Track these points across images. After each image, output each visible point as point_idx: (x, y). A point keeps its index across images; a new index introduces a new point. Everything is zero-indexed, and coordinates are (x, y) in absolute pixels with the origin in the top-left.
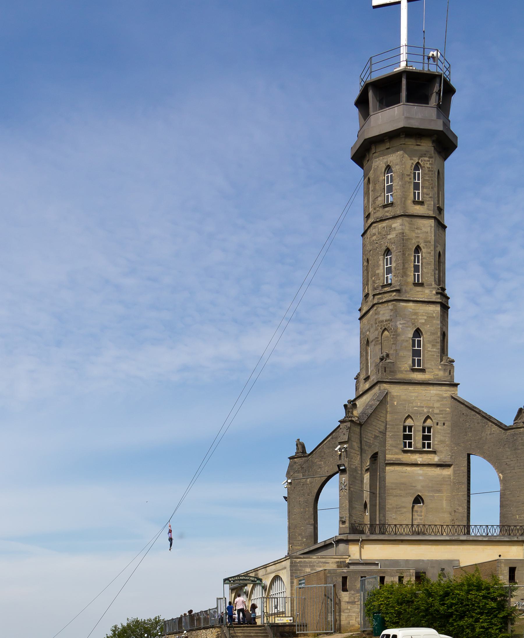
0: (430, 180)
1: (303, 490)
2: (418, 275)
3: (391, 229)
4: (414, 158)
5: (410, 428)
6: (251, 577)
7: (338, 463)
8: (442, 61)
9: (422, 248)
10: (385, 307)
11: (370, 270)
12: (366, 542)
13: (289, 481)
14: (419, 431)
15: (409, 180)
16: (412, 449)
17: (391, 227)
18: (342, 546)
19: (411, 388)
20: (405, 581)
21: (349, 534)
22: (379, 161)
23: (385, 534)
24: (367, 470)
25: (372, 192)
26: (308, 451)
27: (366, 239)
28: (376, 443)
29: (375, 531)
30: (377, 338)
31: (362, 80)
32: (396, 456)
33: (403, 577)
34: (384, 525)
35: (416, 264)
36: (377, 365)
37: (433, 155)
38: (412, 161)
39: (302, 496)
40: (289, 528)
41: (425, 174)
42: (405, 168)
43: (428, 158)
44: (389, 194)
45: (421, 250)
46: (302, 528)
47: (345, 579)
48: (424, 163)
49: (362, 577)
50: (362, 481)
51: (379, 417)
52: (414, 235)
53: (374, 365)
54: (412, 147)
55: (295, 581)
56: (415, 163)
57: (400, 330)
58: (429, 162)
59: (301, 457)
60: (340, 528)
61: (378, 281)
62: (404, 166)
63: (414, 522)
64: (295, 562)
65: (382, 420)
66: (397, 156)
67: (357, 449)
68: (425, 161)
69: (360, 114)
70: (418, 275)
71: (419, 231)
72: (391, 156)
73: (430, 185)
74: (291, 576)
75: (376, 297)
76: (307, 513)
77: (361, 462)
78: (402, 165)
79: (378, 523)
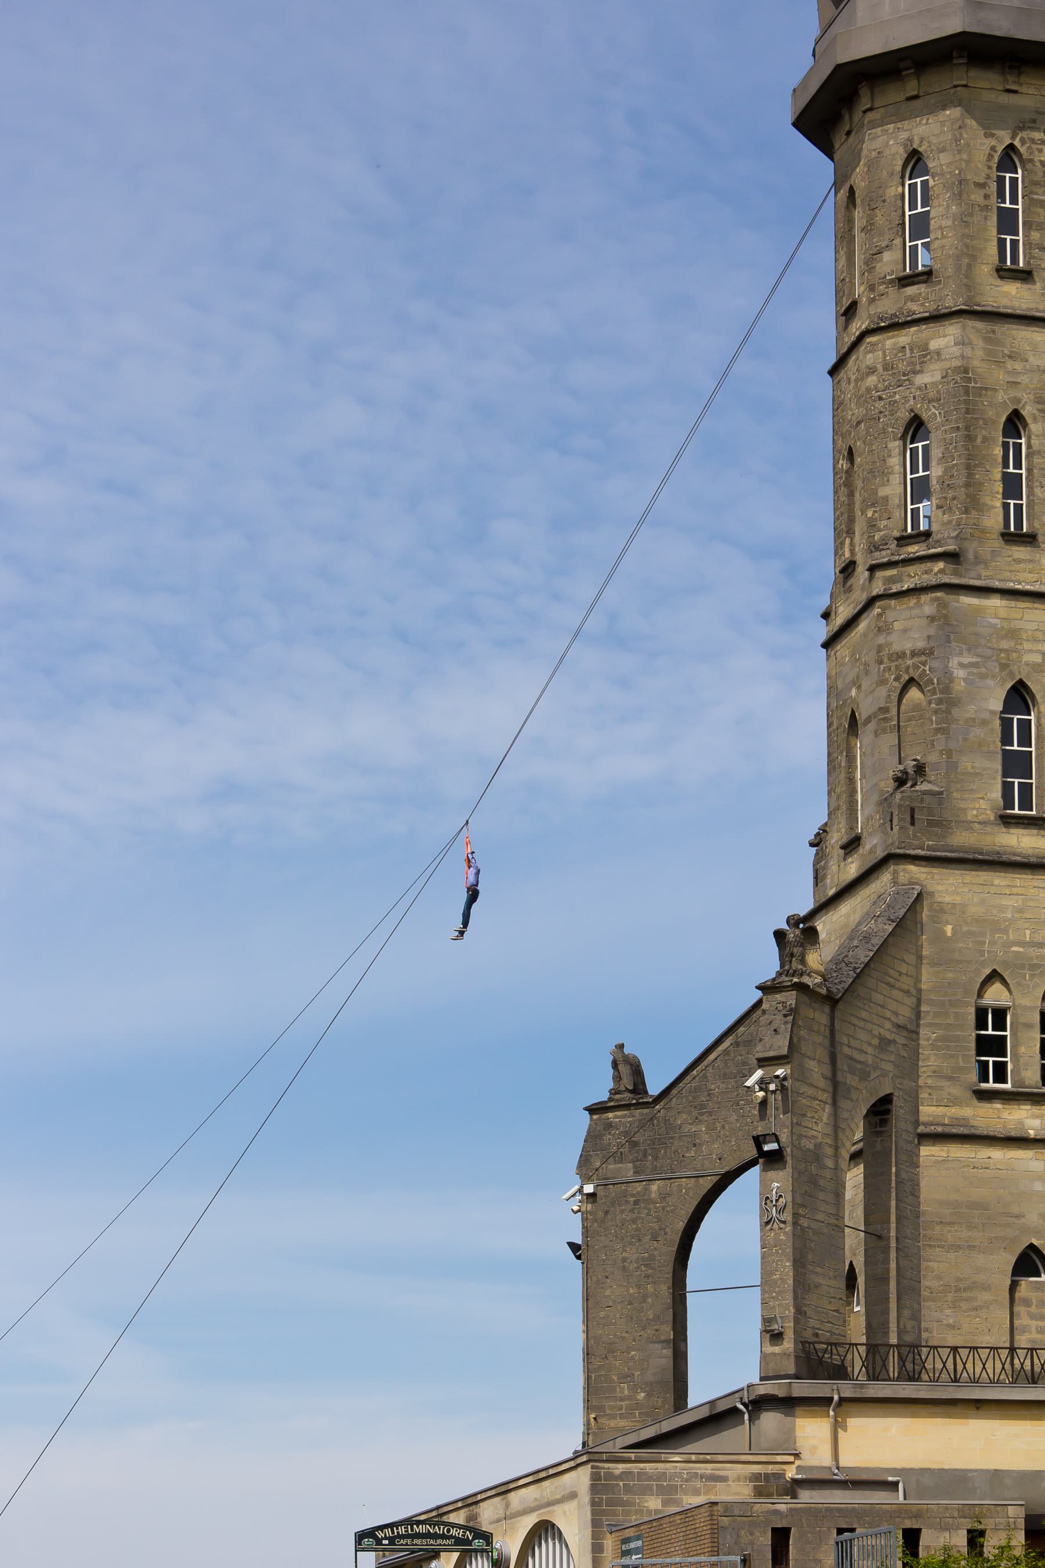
1: (634, 1221)
2: (1018, 508)
3: (925, 355)
4: (1000, 133)
5: (1000, 1016)
6: (453, 1525)
7: (755, 1129)
9: (1029, 420)
10: (911, 608)
11: (859, 484)
12: (853, 1408)
13: (589, 1189)
14: (1029, 1026)
16: (1008, 1086)
17: (925, 347)
18: (770, 1420)
19: (1000, 879)
20: (991, 1545)
21: (797, 1377)
22: (885, 136)
23: (919, 1379)
24: (855, 1157)
25: (863, 234)
26: (654, 1086)
27: (843, 384)
28: (883, 1065)
29: (884, 1371)
30: (886, 710)
32: (954, 1111)
33: (982, 1533)
34: (915, 1347)
35: (1011, 470)
36: (885, 802)
38: (993, 142)
39: (631, 1243)
40: (588, 1354)
41: (1037, 183)
42: (968, 162)
43: (1042, 134)
44: (919, 242)
45: (1025, 425)
46: (633, 1353)
47: (781, 1537)
48: (1029, 148)
49: (840, 1531)
50: (838, 1194)
51: (895, 974)
52: (1002, 377)
53: (875, 798)
54: (992, 96)
55: (609, 1543)
56: (1000, 148)
57: (959, 686)
59: (627, 1107)
60: (764, 1357)
61: (884, 523)
62: (965, 157)
63: (1017, 1338)
64: (609, 1476)
65: (905, 987)
66: (943, 123)
67: (822, 1083)
68: (1033, 141)
70: (1018, 508)
71: (1018, 366)
72: (924, 121)
74: (596, 1523)
75: (880, 574)
76: (650, 1300)
77: (836, 1128)
78: (960, 152)
79: (893, 1340)
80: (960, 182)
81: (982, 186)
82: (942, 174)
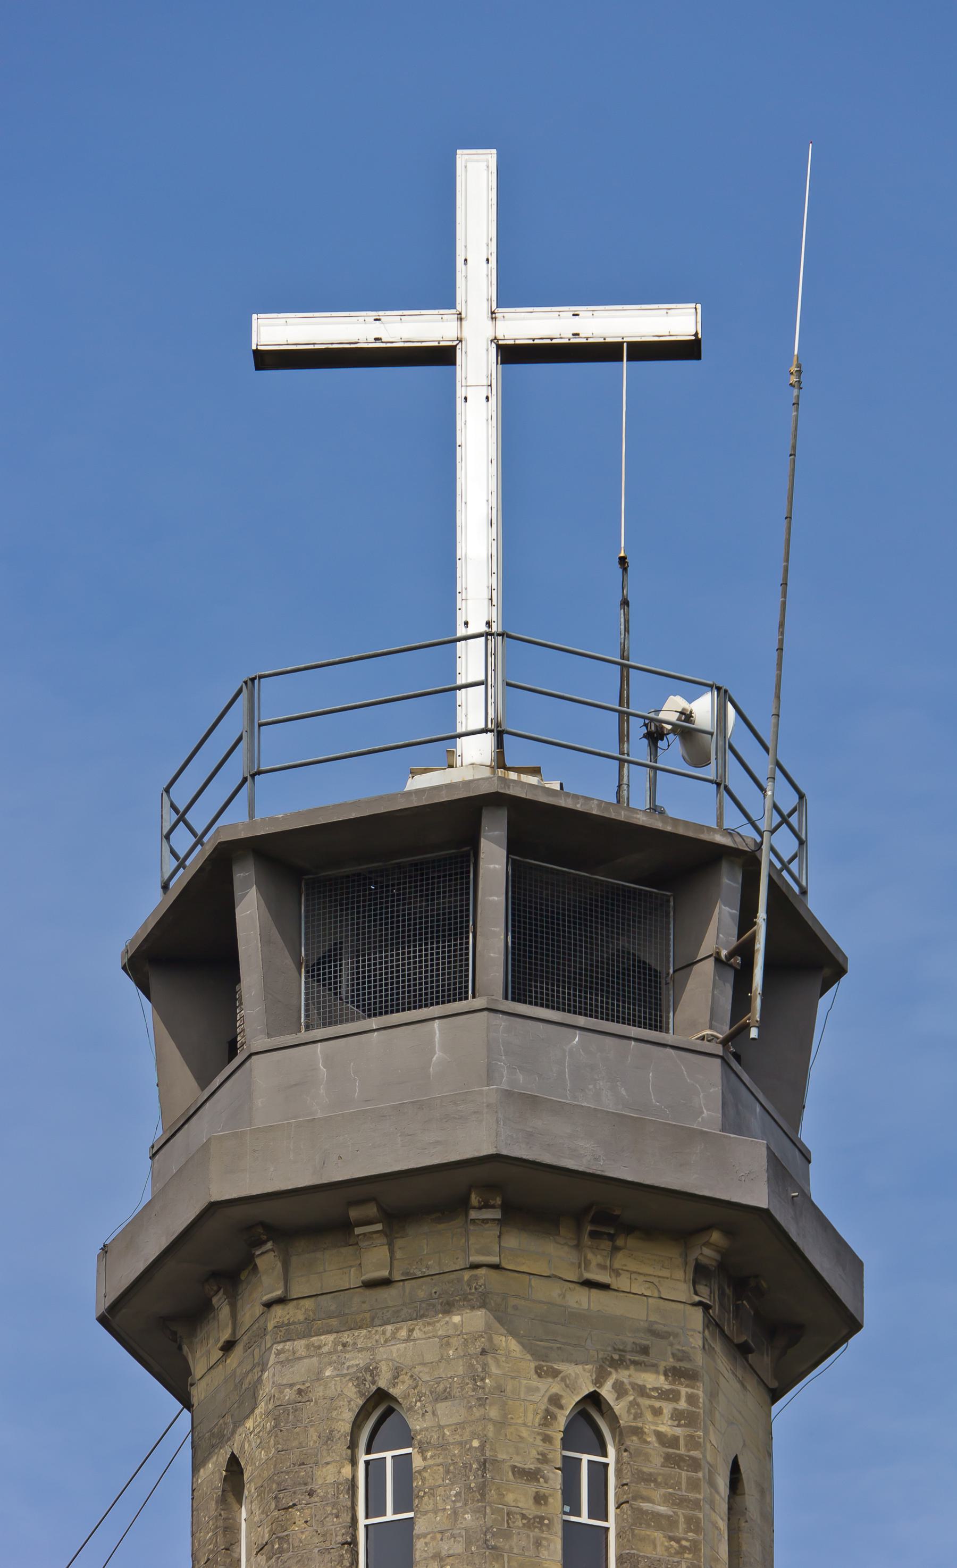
0: (677, 1522)
8: (761, 765)
15: (532, 1510)
22: (315, 1360)
25: (262, 1559)
31: (182, 818)
37: (699, 1359)
38: (556, 1387)
42: (501, 1424)
43: (662, 1378)
48: (634, 1404)
54: (553, 1292)
56: (571, 1401)
58: (667, 1399)
62: (494, 1413)
66: (445, 1341)
68: (642, 1391)
69: (171, 1047)
72: (403, 1333)
73: (677, 1553)
78: (482, 1402)
80: (483, 1465)
81: (532, 1476)
82: (443, 1446)
